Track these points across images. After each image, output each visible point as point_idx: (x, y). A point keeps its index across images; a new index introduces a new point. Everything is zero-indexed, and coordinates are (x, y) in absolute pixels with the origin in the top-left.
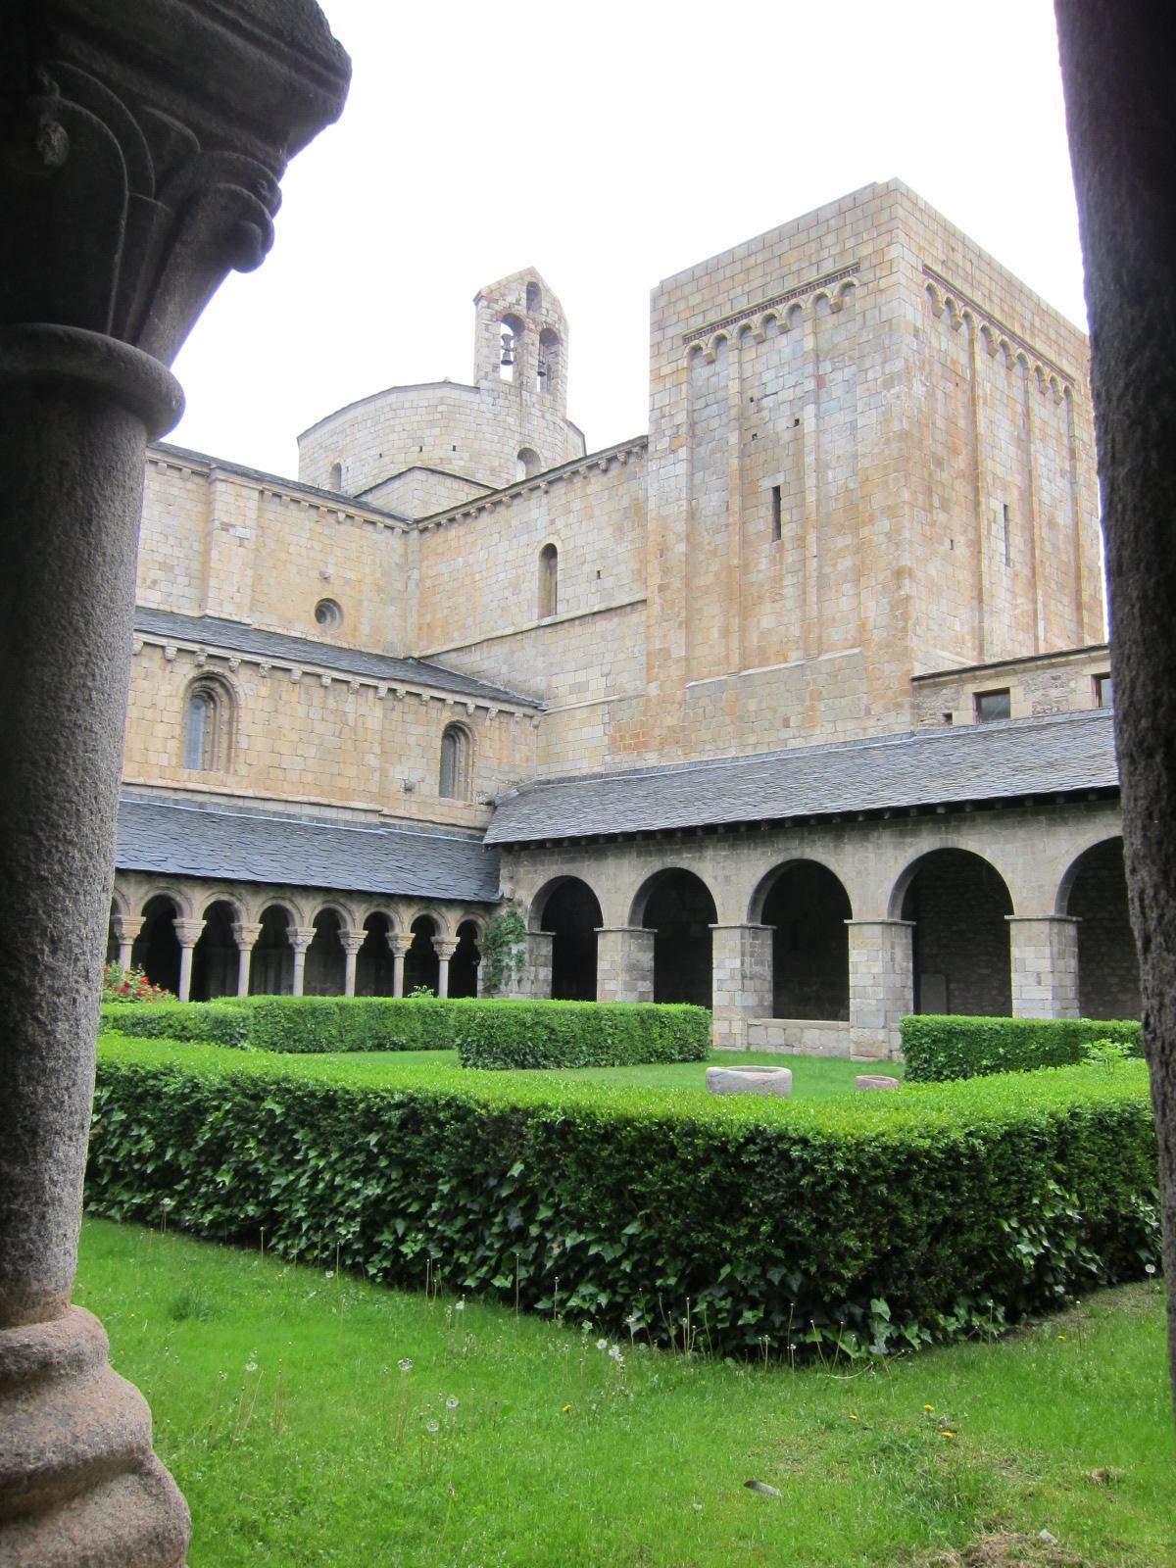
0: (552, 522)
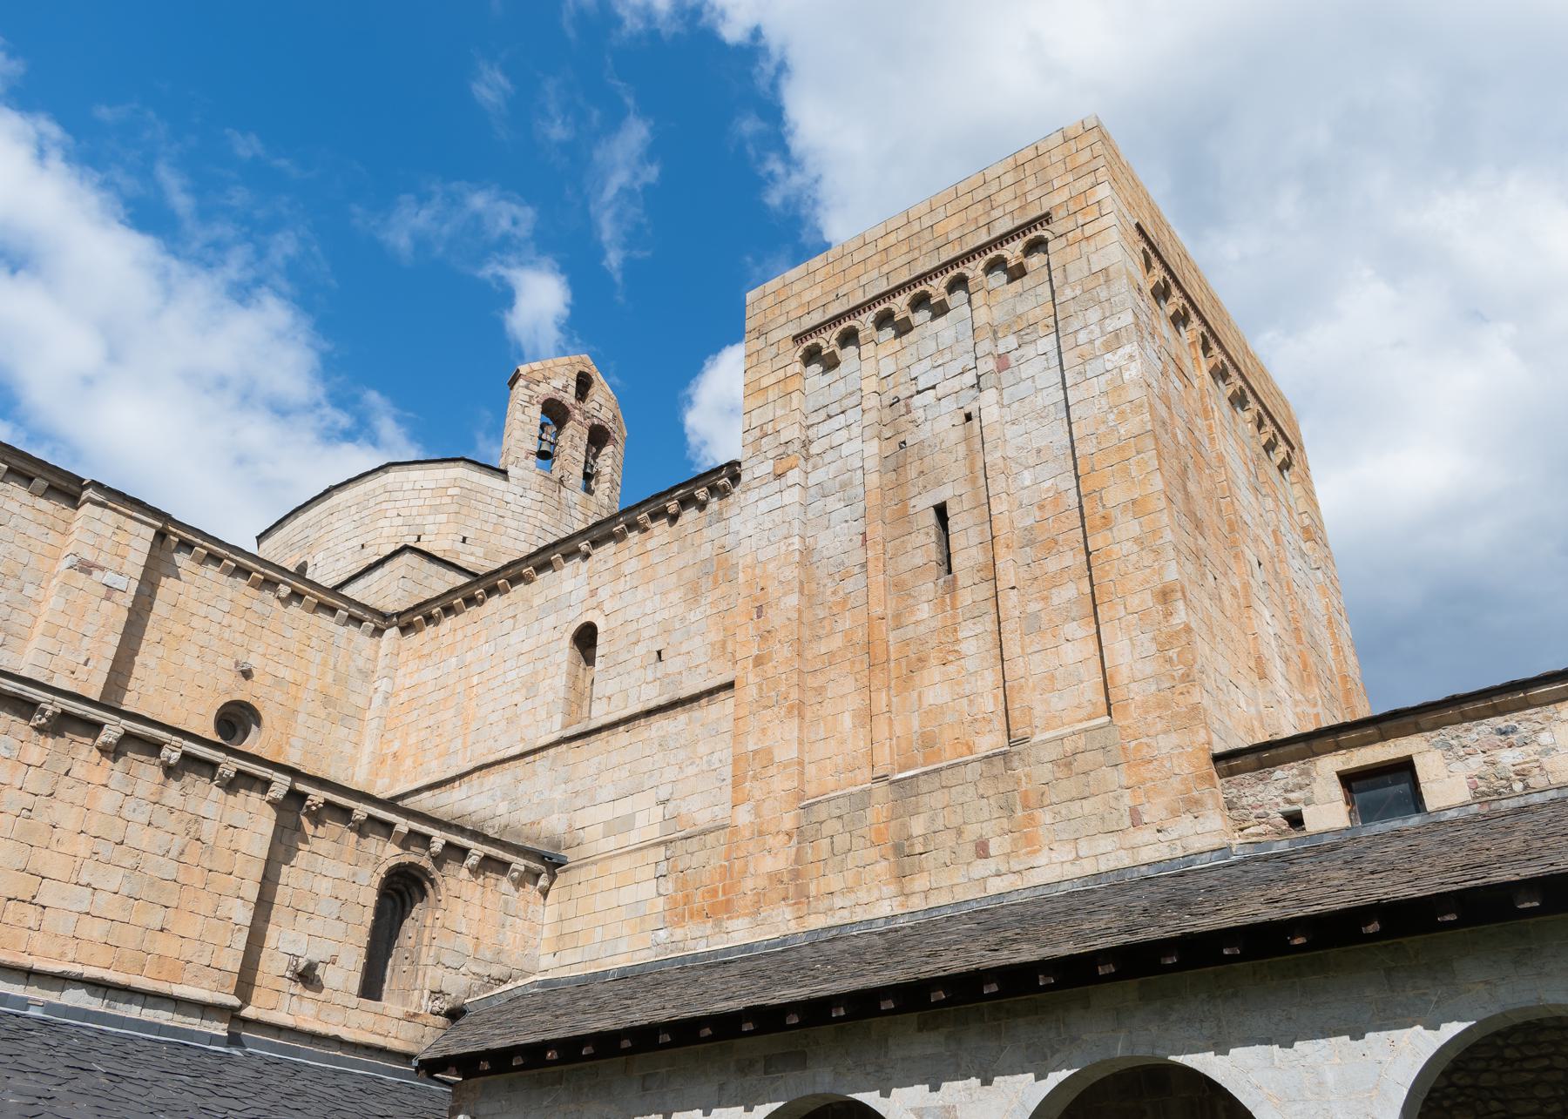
0: (593, 593)
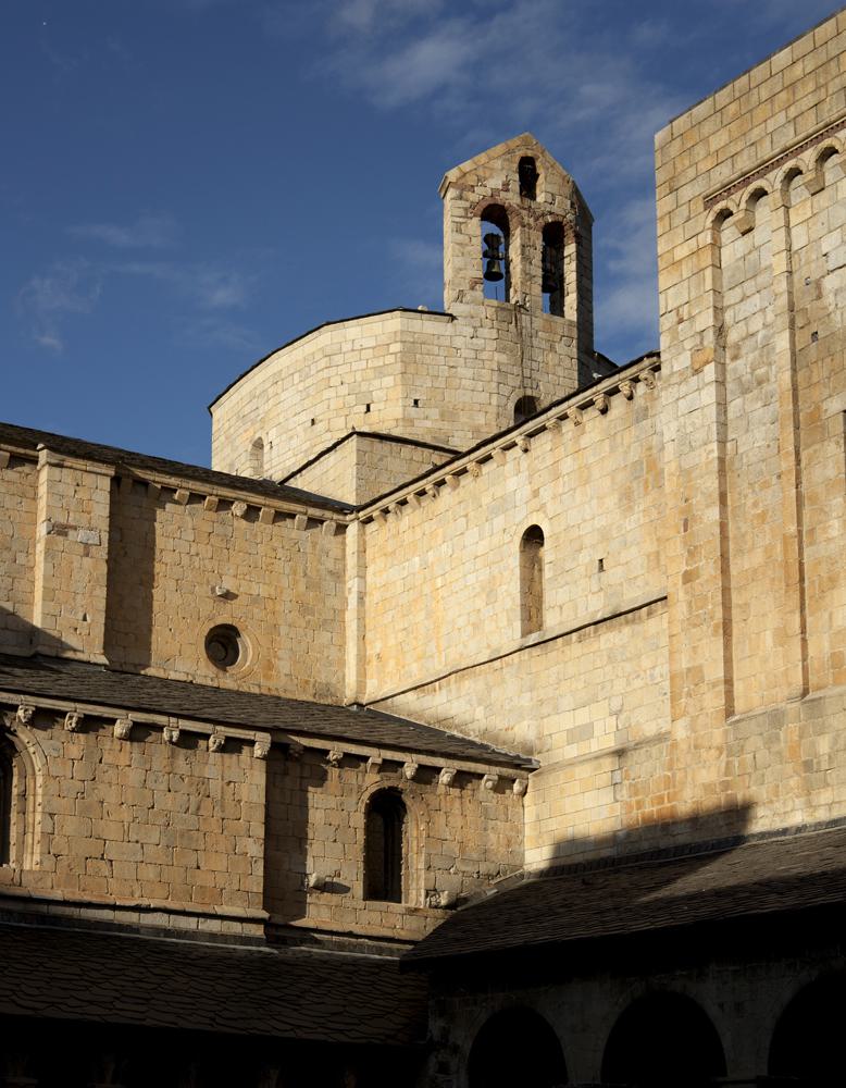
0: (536, 493)
